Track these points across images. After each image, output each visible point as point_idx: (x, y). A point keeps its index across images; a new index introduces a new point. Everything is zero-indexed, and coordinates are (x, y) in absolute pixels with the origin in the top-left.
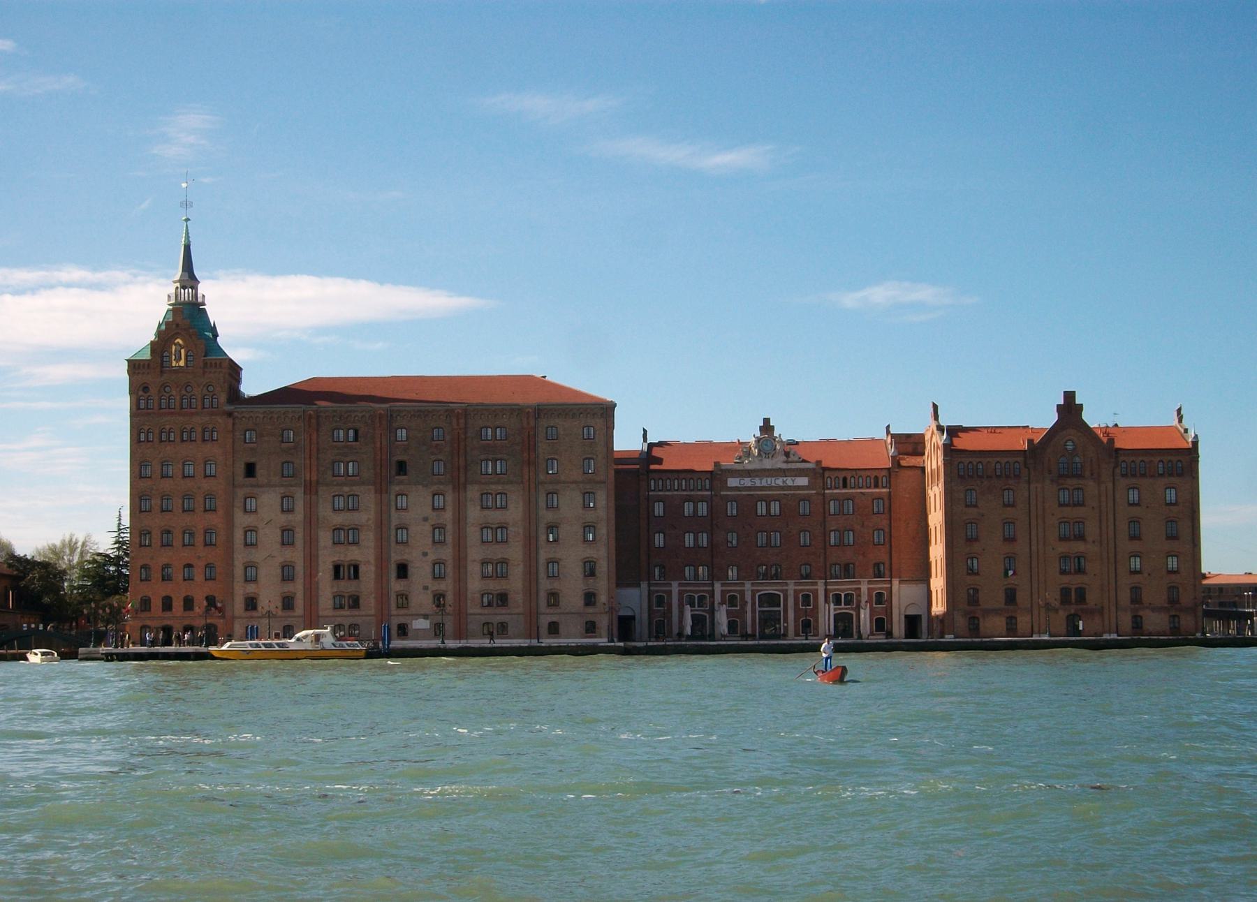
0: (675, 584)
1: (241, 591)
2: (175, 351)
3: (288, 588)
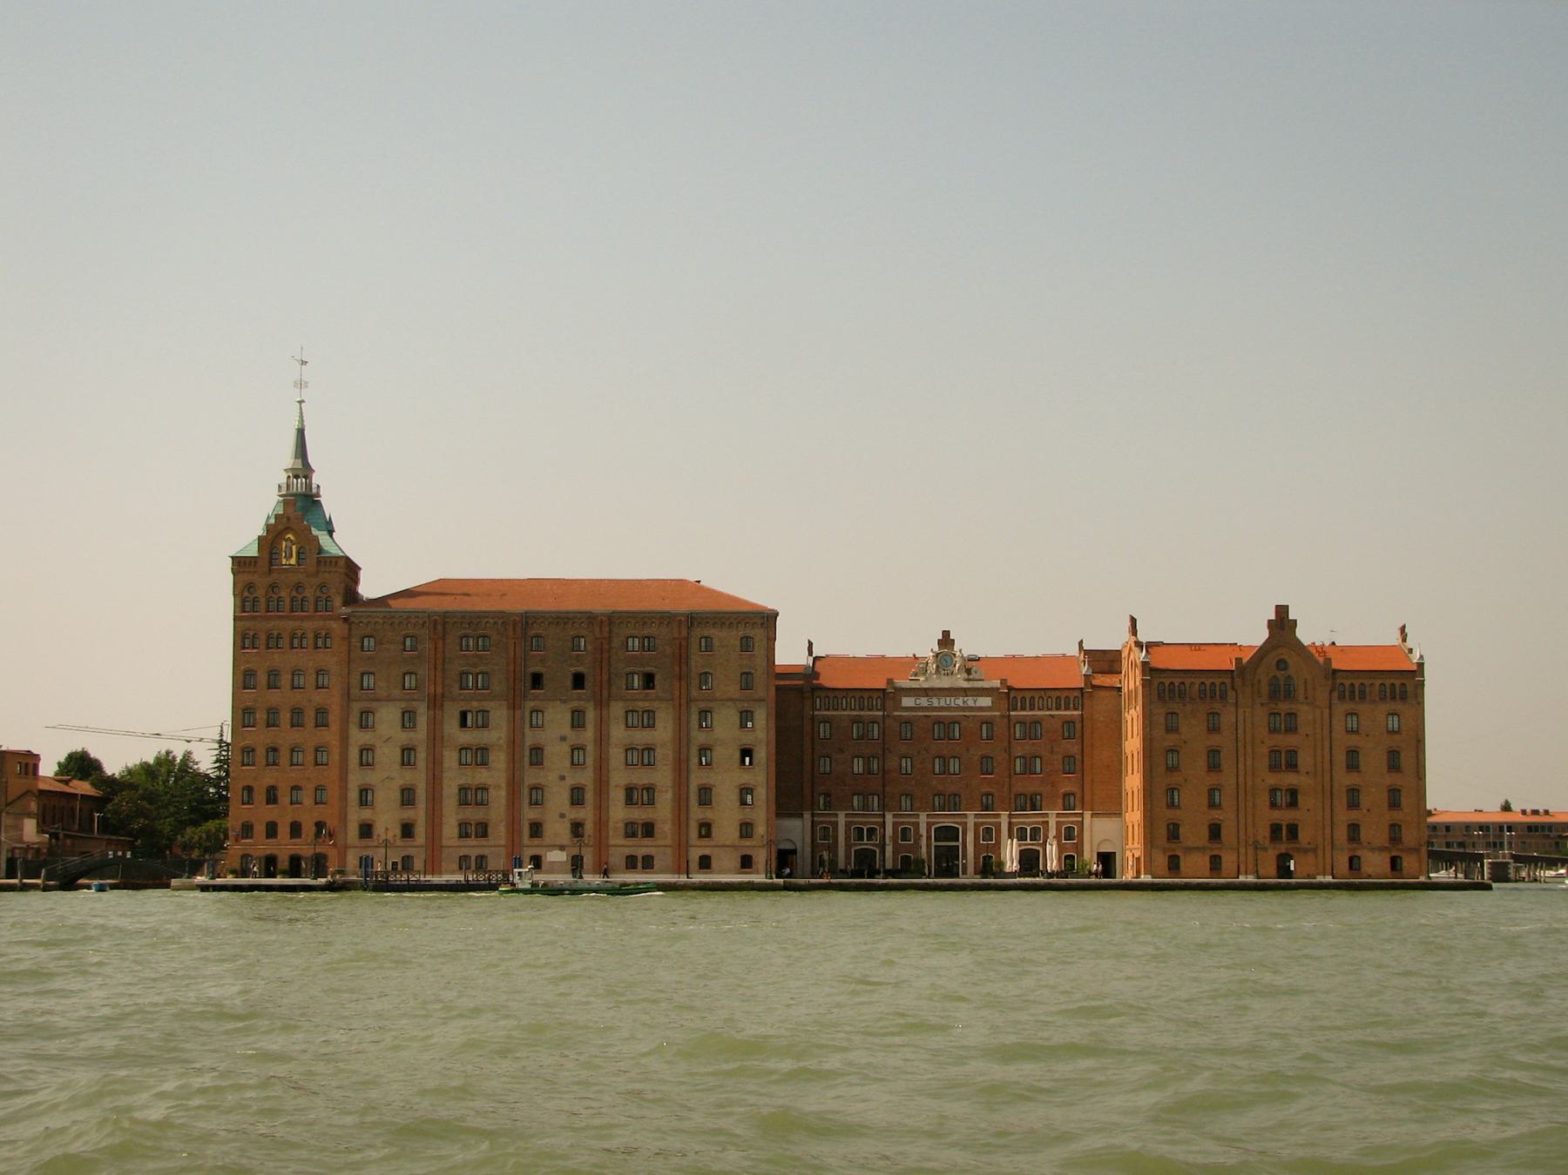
1: (356, 816)
2: (286, 547)
3: (408, 814)
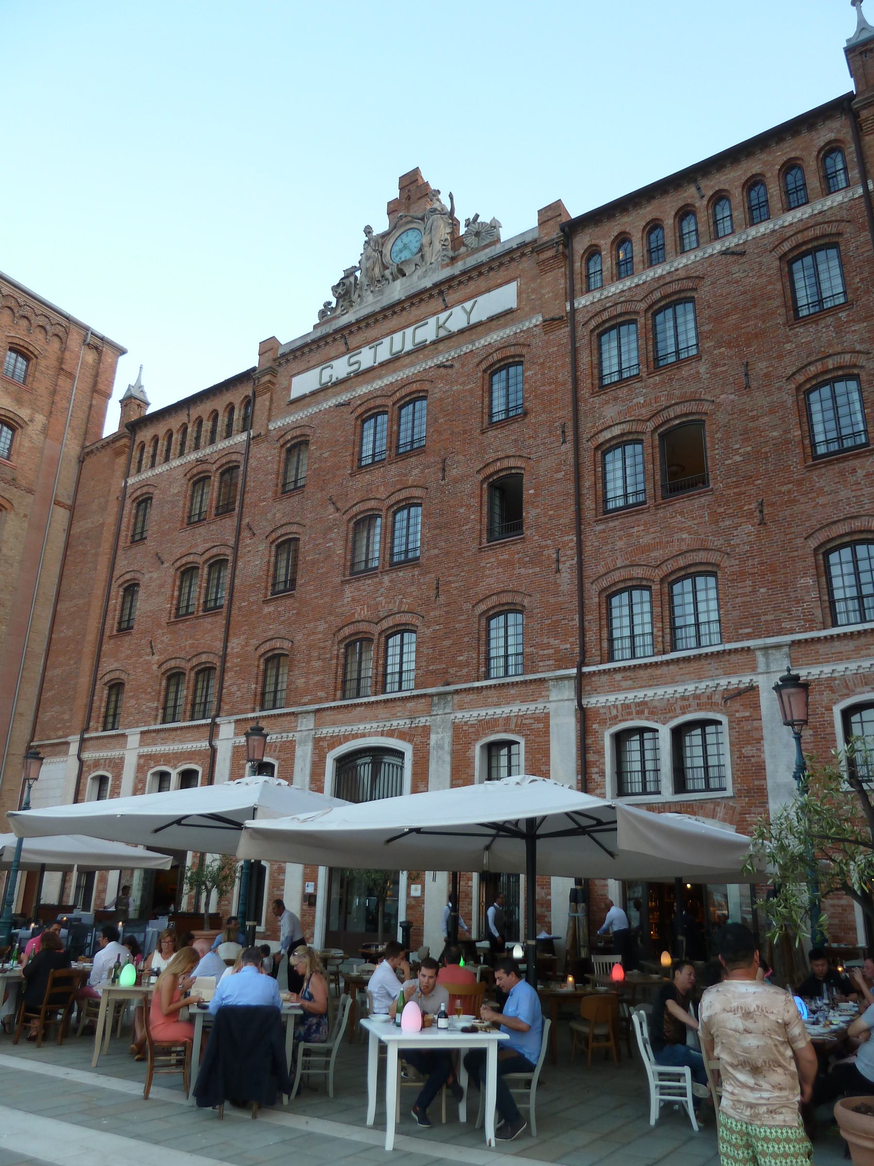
0: (133, 739)
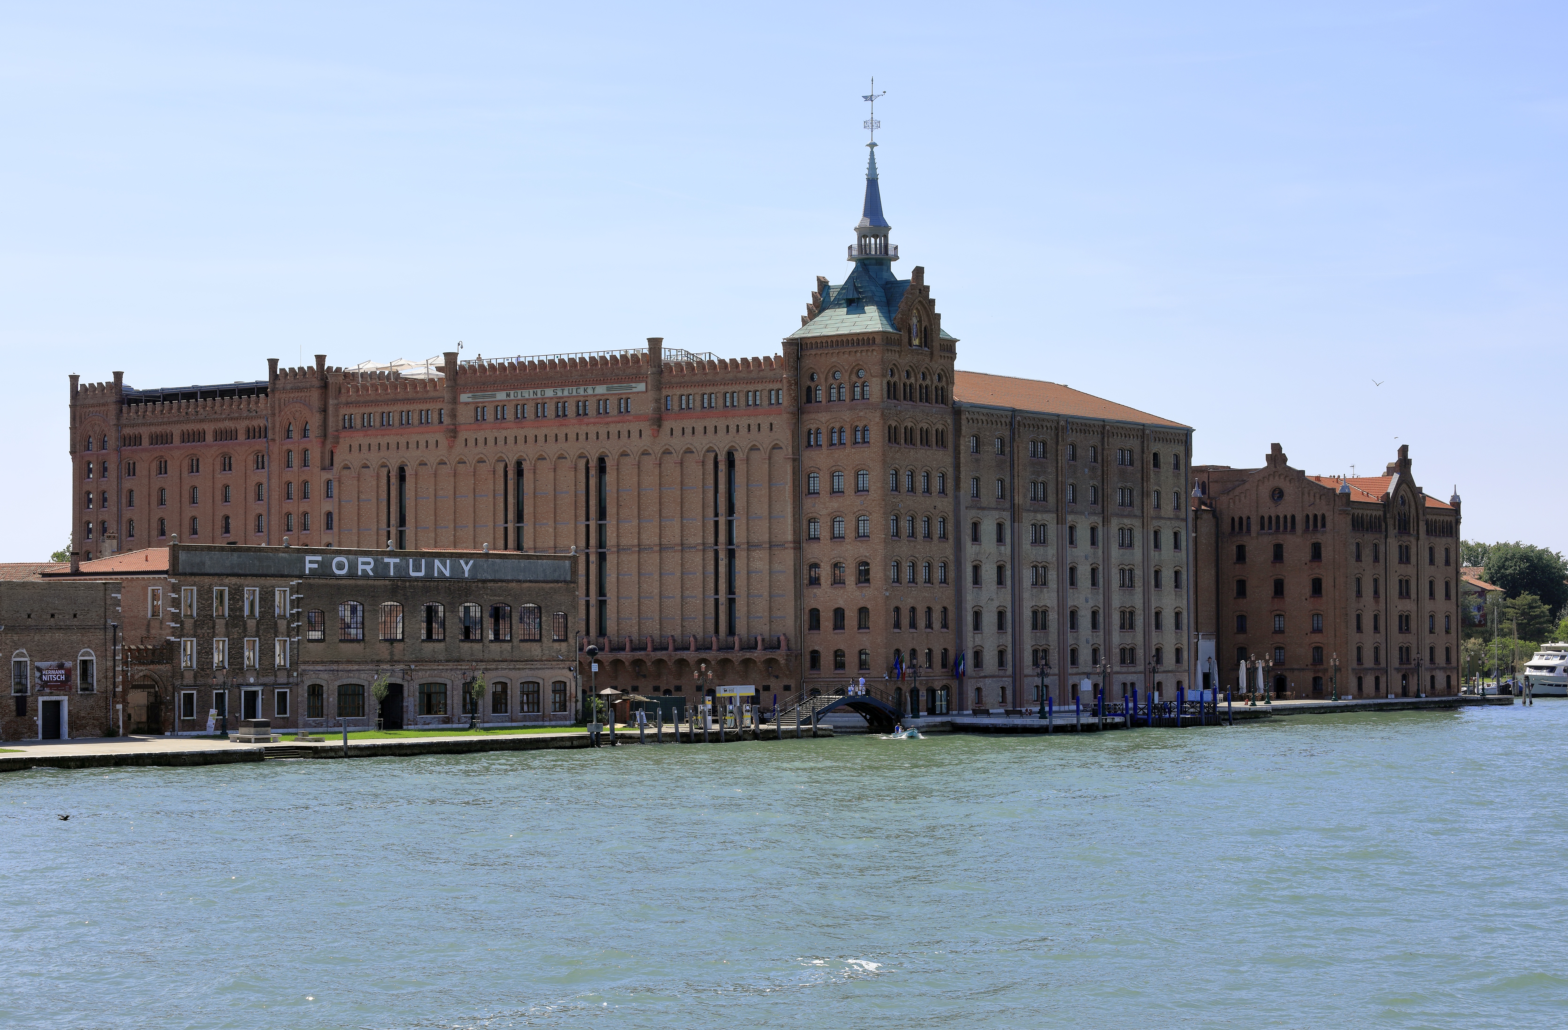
1: (971, 641)
